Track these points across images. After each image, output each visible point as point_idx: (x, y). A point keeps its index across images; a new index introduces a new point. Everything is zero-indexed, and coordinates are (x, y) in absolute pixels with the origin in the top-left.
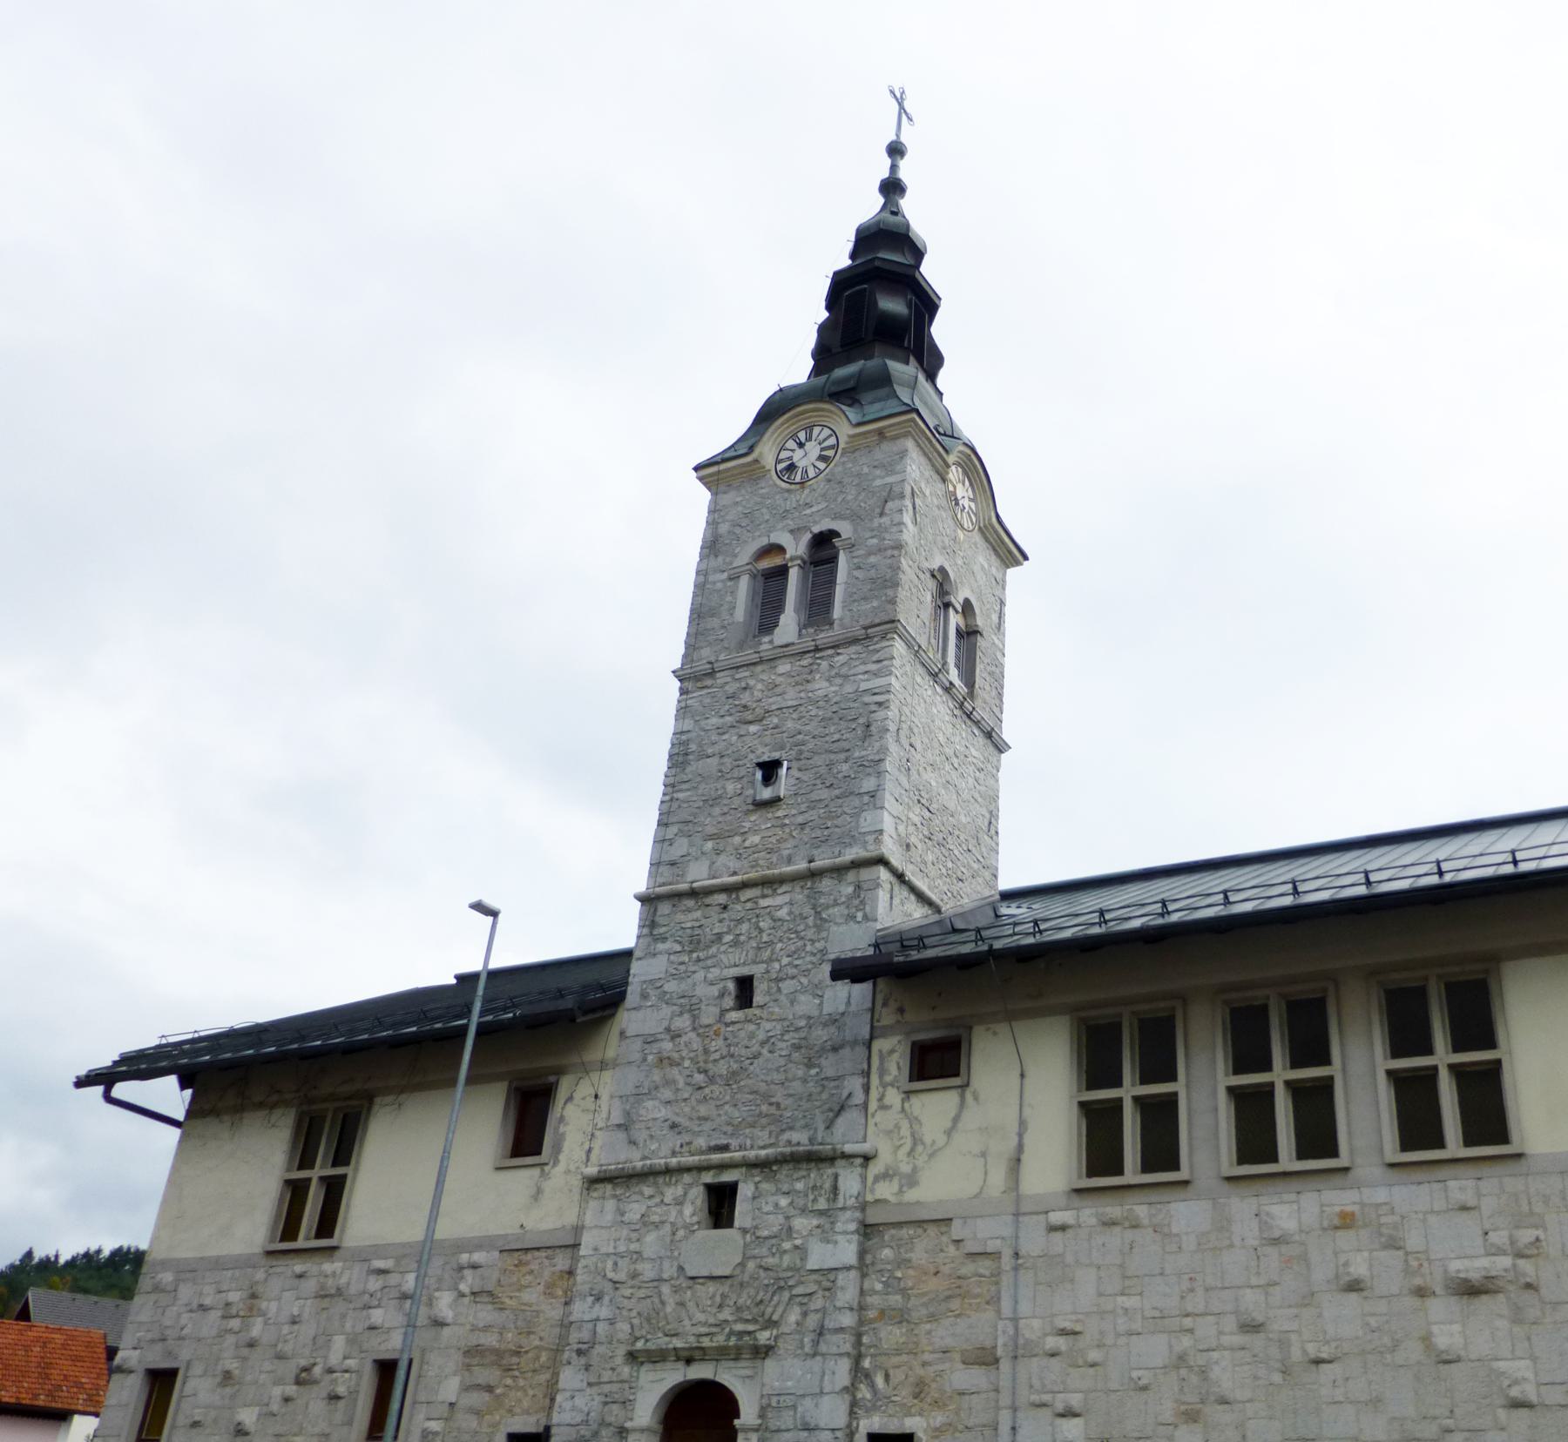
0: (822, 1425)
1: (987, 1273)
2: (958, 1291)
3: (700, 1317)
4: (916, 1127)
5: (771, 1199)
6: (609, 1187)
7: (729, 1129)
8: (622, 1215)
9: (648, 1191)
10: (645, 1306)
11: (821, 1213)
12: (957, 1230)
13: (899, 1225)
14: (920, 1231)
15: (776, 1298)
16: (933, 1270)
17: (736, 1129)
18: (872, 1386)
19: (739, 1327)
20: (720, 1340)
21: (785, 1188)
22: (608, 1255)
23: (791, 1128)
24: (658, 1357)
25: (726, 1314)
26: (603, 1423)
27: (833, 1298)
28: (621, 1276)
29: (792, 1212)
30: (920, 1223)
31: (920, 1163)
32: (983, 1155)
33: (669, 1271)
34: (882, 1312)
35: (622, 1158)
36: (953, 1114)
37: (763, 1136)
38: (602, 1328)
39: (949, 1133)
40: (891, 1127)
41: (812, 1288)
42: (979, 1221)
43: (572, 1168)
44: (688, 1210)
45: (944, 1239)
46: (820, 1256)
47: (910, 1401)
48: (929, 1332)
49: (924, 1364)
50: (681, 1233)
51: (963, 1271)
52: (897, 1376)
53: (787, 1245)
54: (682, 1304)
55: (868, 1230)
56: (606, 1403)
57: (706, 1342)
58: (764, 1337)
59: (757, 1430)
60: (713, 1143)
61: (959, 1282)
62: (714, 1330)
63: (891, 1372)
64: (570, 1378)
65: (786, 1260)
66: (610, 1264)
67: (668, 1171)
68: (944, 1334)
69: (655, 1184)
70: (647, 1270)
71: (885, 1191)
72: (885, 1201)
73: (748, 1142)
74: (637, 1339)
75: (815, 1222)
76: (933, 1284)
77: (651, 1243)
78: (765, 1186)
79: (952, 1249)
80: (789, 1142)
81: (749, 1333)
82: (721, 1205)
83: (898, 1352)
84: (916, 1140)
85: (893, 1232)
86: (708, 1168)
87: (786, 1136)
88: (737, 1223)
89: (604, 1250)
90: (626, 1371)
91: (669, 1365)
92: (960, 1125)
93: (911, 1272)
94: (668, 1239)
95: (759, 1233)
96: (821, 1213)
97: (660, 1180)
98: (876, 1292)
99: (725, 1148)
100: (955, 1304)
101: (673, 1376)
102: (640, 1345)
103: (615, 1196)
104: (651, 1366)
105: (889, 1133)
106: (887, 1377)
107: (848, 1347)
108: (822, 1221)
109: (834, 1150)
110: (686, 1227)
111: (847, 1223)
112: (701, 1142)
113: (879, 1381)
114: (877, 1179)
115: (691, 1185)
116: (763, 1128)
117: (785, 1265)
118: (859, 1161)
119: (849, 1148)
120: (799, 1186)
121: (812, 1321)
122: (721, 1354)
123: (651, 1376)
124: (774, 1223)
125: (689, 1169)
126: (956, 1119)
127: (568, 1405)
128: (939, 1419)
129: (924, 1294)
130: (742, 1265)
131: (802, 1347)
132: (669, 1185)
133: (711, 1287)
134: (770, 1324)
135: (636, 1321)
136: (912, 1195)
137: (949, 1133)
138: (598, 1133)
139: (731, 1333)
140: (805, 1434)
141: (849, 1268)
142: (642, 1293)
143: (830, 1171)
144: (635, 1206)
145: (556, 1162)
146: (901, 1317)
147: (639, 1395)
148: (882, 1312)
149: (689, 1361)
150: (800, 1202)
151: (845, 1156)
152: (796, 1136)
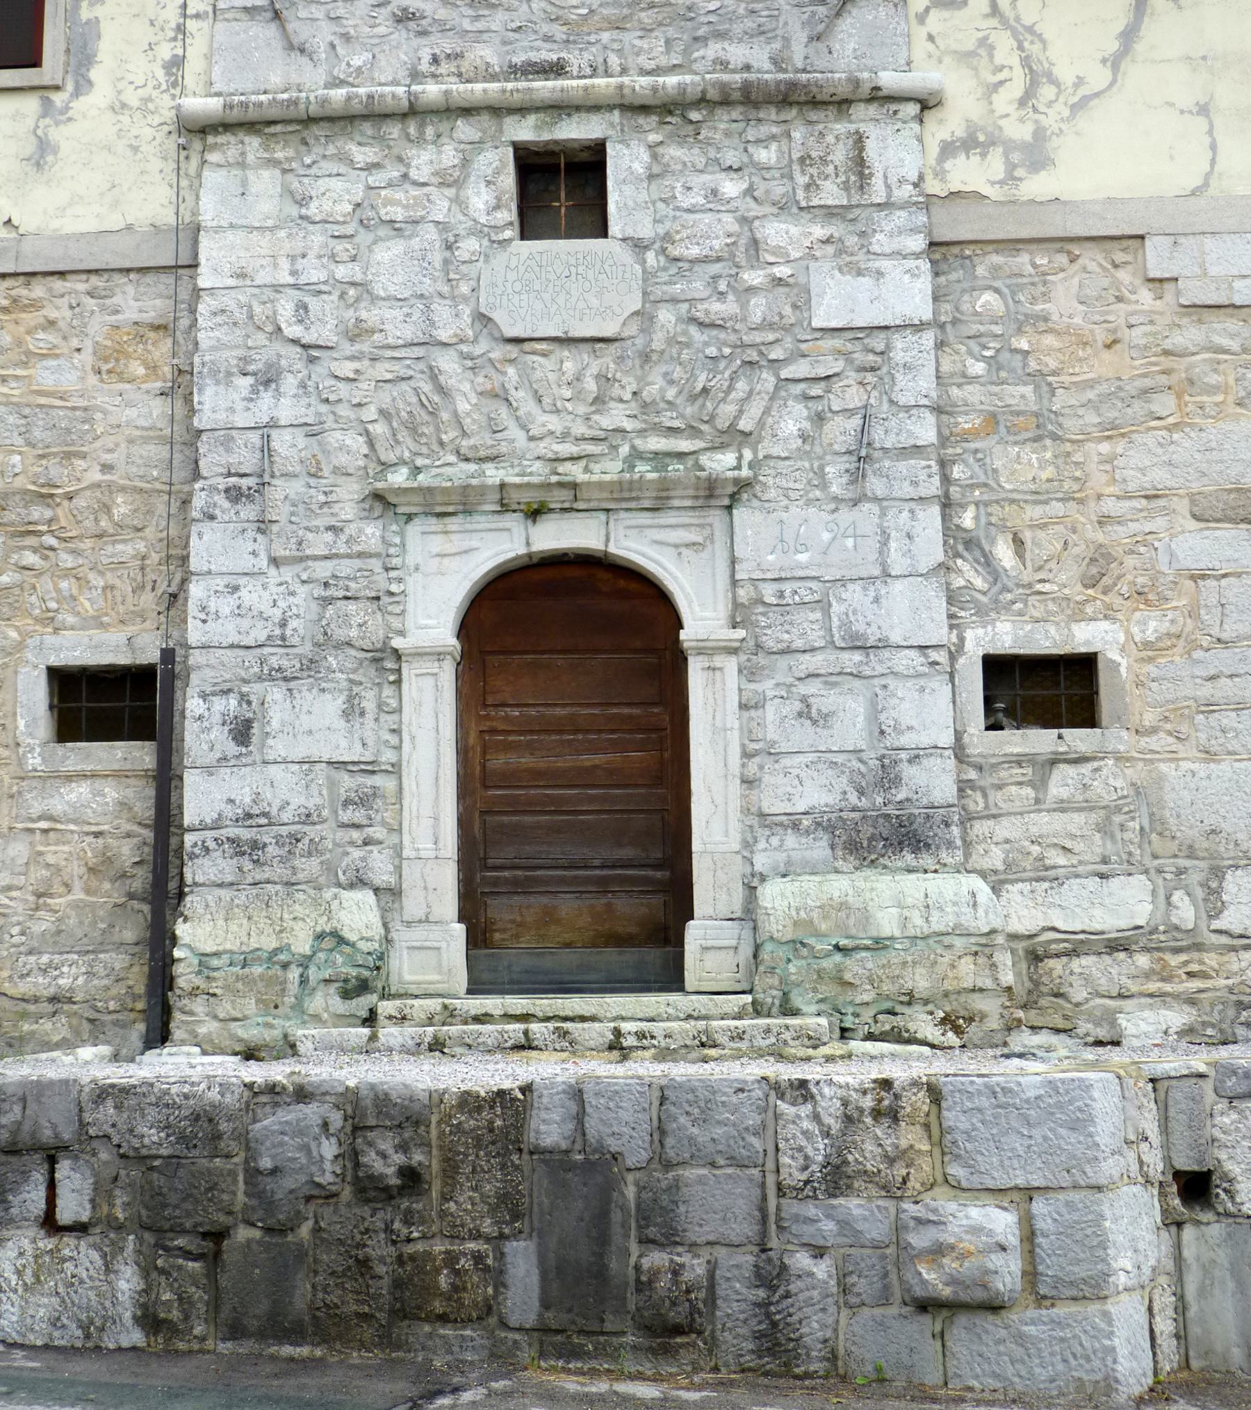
0: (896, 638)
1: (1235, 345)
2: (1163, 380)
3: (555, 423)
4: (1034, 49)
5: (697, 180)
6: (253, 143)
7: (559, 31)
8: (303, 201)
9: (362, 154)
10: (402, 398)
11: (830, 213)
12: (1157, 258)
13: (1014, 245)
14: (1062, 259)
15: (742, 386)
16: (1101, 336)
17: (576, 30)
18: (987, 562)
19: (656, 443)
20: (609, 470)
21: (731, 157)
22: (277, 288)
23: (721, 35)
24: (451, 506)
25: (617, 416)
26: (327, 641)
27: (886, 387)
28: (324, 333)
29: (754, 210)
30: (1064, 243)
31: (1050, 120)
32: (1203, 110)
33: (450, 322)
34: (992, 420)
35: (276, 80)
36: (1120, 26)
37: (654, 49)
38: (282, 442)
39: (1115, 63)
40: (970, 45)
41: (837, 366)
42: (1209, 242)
43: (132, 98)
44: (479, 199)
45: (1124, 275)
46: (837, 300)
47: (1077, 592)
48: (1110, 460)
49: (1104, 521)
50: (469, 246)
51: (1177, 340)
52: (1044, 544)
53: (753, 277)
54: (500, 396)
55: (940, 250)
56: (327, 601)
57: (575, 472)
58: (722, 463)
59: (734, 651)
60: (518, 59)
61: (1167, 362)
62: (590, 448)
63: (1027, 536)
64: (216, 547)
65: (758, 308)
66: (285, 309)
67: (413, 111)
68: (1142, 461)
69: (380, 139)
70: (397, 326)
71: (968, 173)
72: (979, 196)
73: (614, 61)
74: (386, 466)
75: (819, 231)
76: (1104, 365)
77: (390, 264)
78: (674, 152)
79: (1145, 296)
80: (723, 65)
81: (681, 456)
82: (560, 188)
83: (1039, 497)
84: (1036, 77)
85: (997, 259)
86: (521, 110)
87: (713, 50)
88: (614, 228)
89: (262, 278)
90: (371, 533)
91: (480, 521)
92: (1139, 47)
93: (1049, 340)
94: (437, 257)
95: (676, 251)
96: (830, 213)
97: (394, 130)
98: (973, 379)
99: (556, 69)
100: (1165, 404)
101: (498, 545)
102: (399, 478)
103: (273, 163)
104: (433, 524)
105: (965, 57)
106: (1018, 543)
107: (933, 486)
108: (835, 229)
109: (857, 83)
110: (478, 231)
111: (900, 235)
112: (487, 54)
113: (1004, 553)
114: (948, 150)
115: (478, 145)
116: (647, 31)
117: (757, 316)
118: (912, 109)
119: (889, 80)
120: (766, 155)
121: (841, 431)
122: (620, 499)
123: (437, 544)
124: (716, 231)
125: (467, 111)
126: (1129, 36)
127: (225, 605)
128: (1153, 626)
129: (1090, 384)
130: (644, 317)
131: (824, 485)
132: (420, 141)
133: (570, 362)
134: (732, 437)
135: (379, 429)
136: (1036, 186)
137: (1115, 63)
138: (191, 25)
139: (637, 455)
140: (857, 657)
141: (919, 327)
142: (383, 370)
143: (841, 127)
144: (337, 184)
145: (83, 85)
146: (1041, 429)
147: (413, 584)
148: (992, 420)
149: (535, 514)
150: (779, 189)
151: (878, 97)
152: (737, 53)
